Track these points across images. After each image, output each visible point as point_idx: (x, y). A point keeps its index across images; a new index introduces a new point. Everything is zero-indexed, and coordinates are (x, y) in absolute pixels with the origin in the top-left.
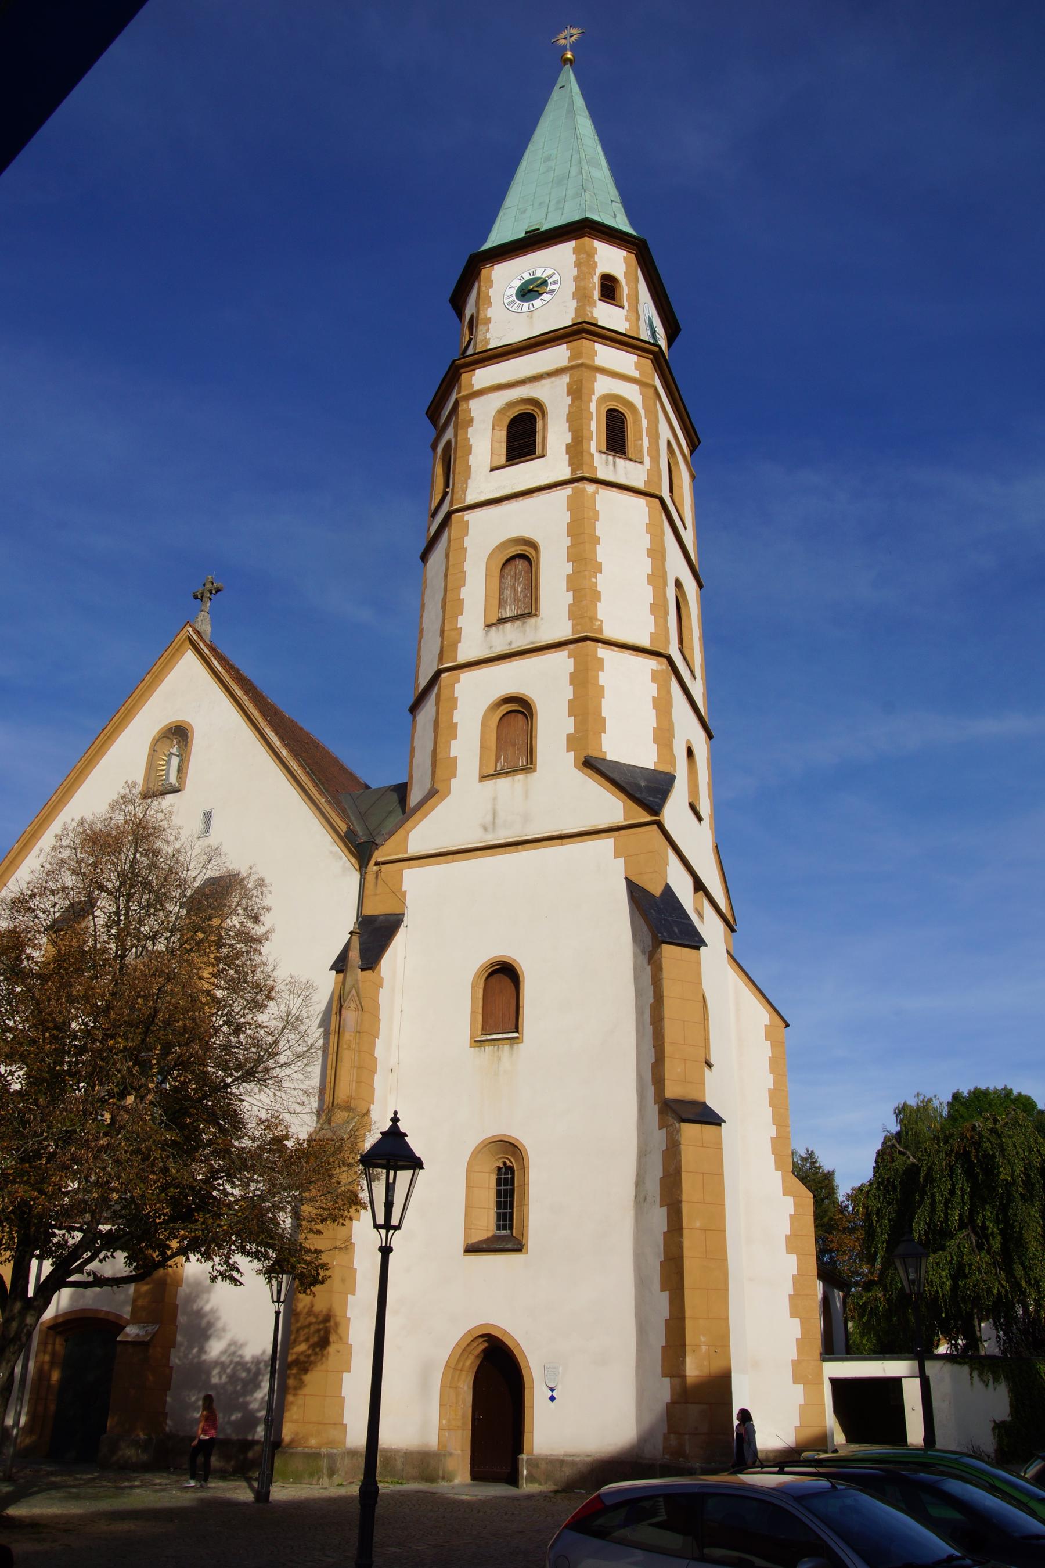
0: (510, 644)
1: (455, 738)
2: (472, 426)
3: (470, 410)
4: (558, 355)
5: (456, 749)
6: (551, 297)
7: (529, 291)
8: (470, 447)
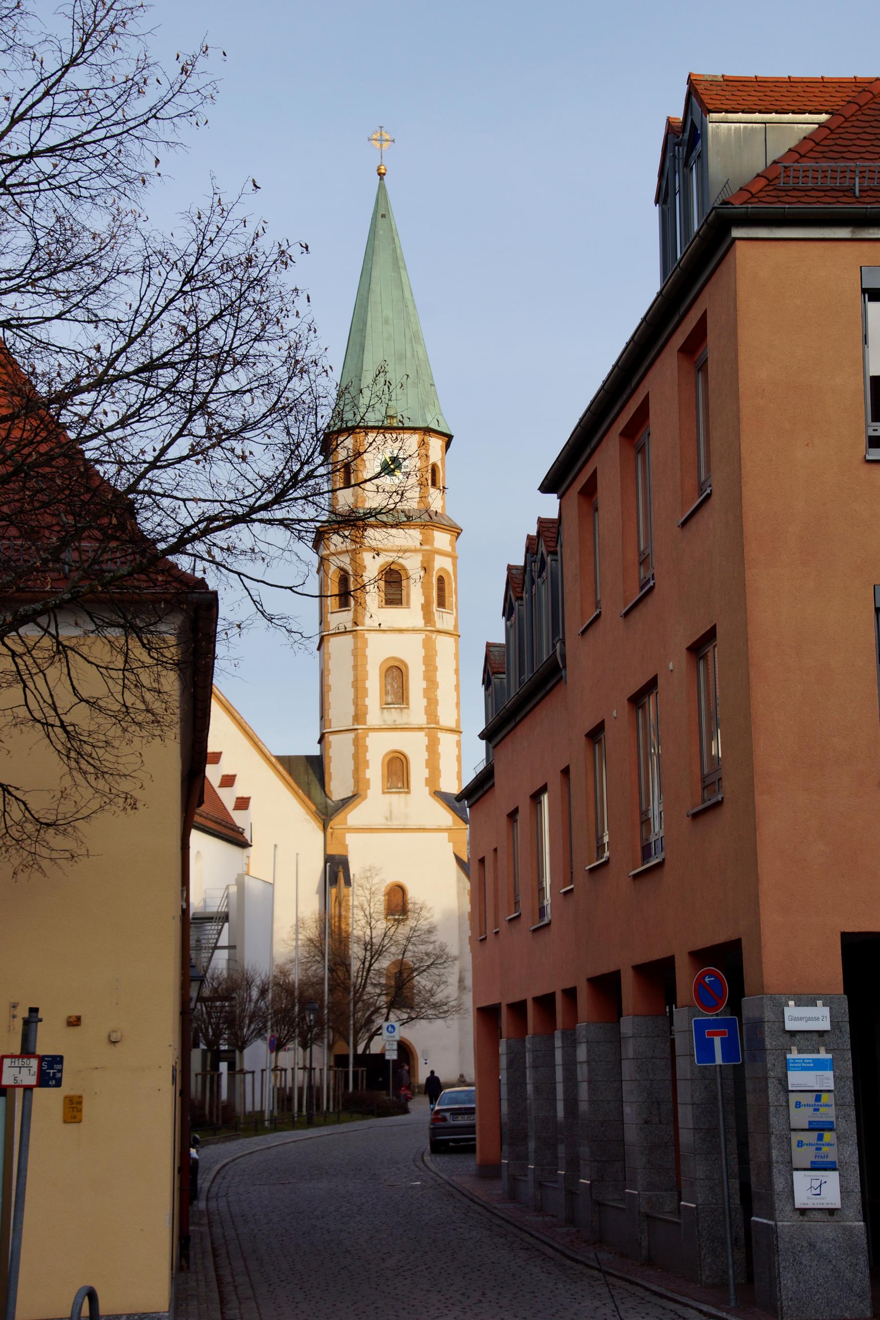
1: (368, 767)
3: (363, 560)
7: (390, 467)
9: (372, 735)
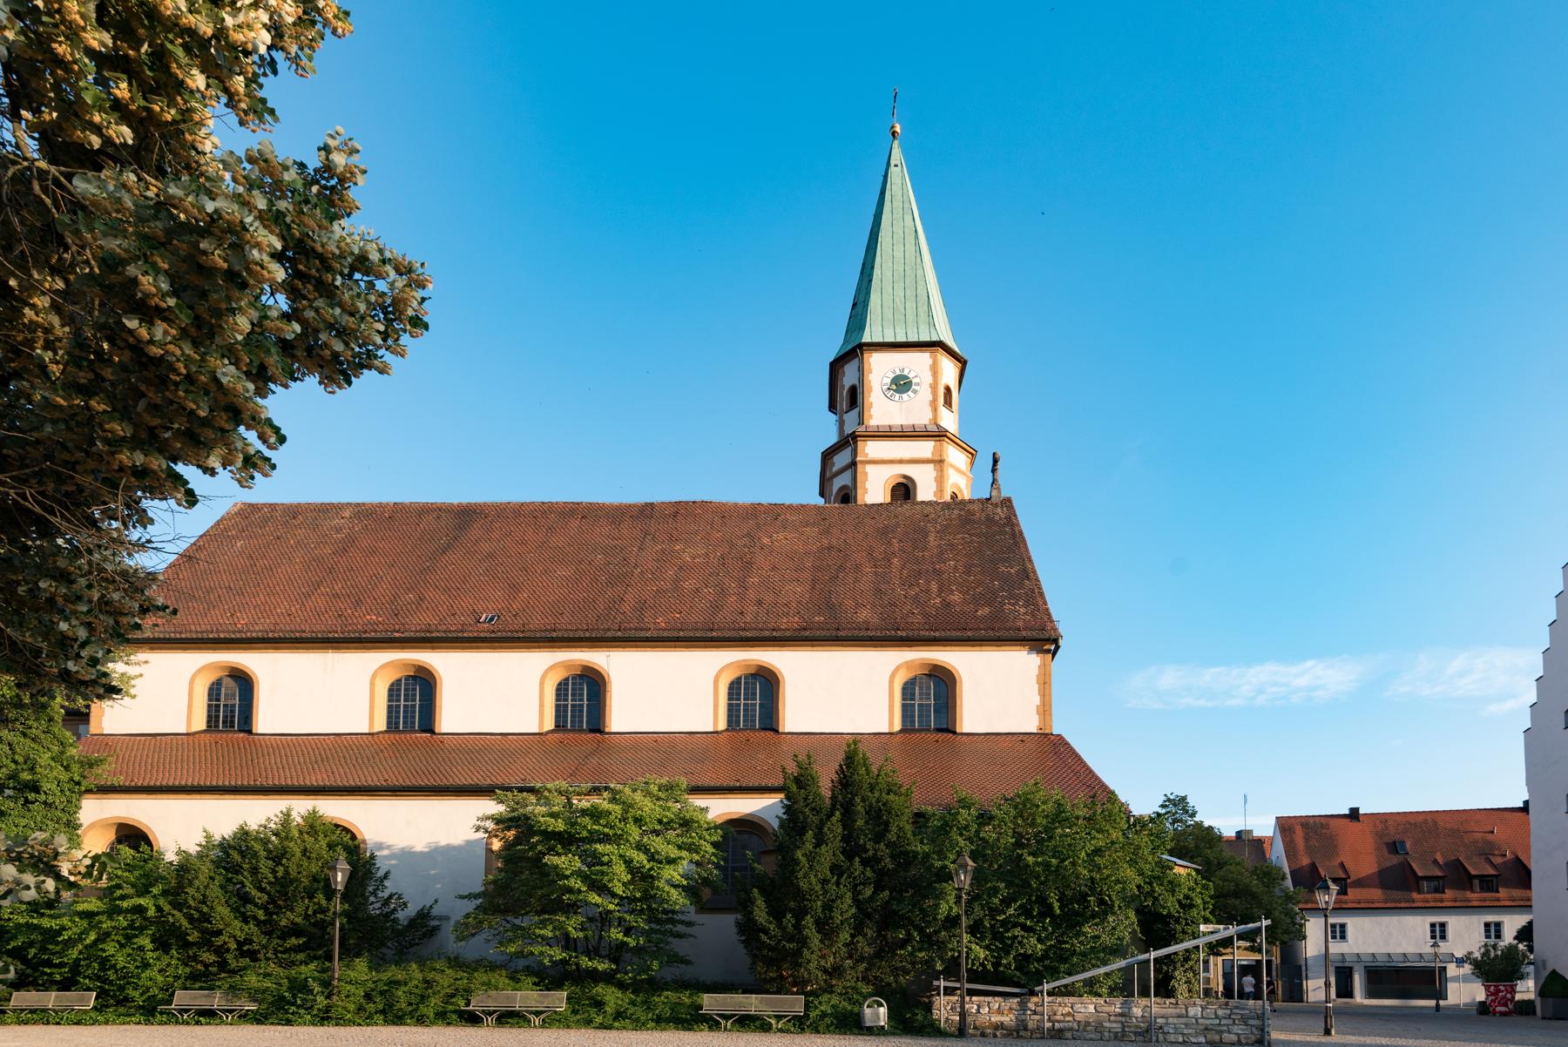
4: (925, 448)
7: (901, 384)
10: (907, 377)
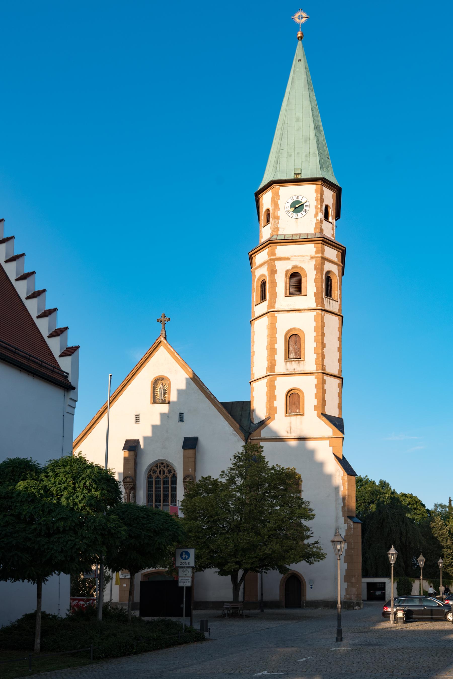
0: (294, 369)
1: (276, 400)
2: (276, 274)
3: (275, 266)
4: (310, 248)
5: (276, 404)
6: (305, 213)
8: (276, 283)
9: (279, 379)
10: (300, 202)
